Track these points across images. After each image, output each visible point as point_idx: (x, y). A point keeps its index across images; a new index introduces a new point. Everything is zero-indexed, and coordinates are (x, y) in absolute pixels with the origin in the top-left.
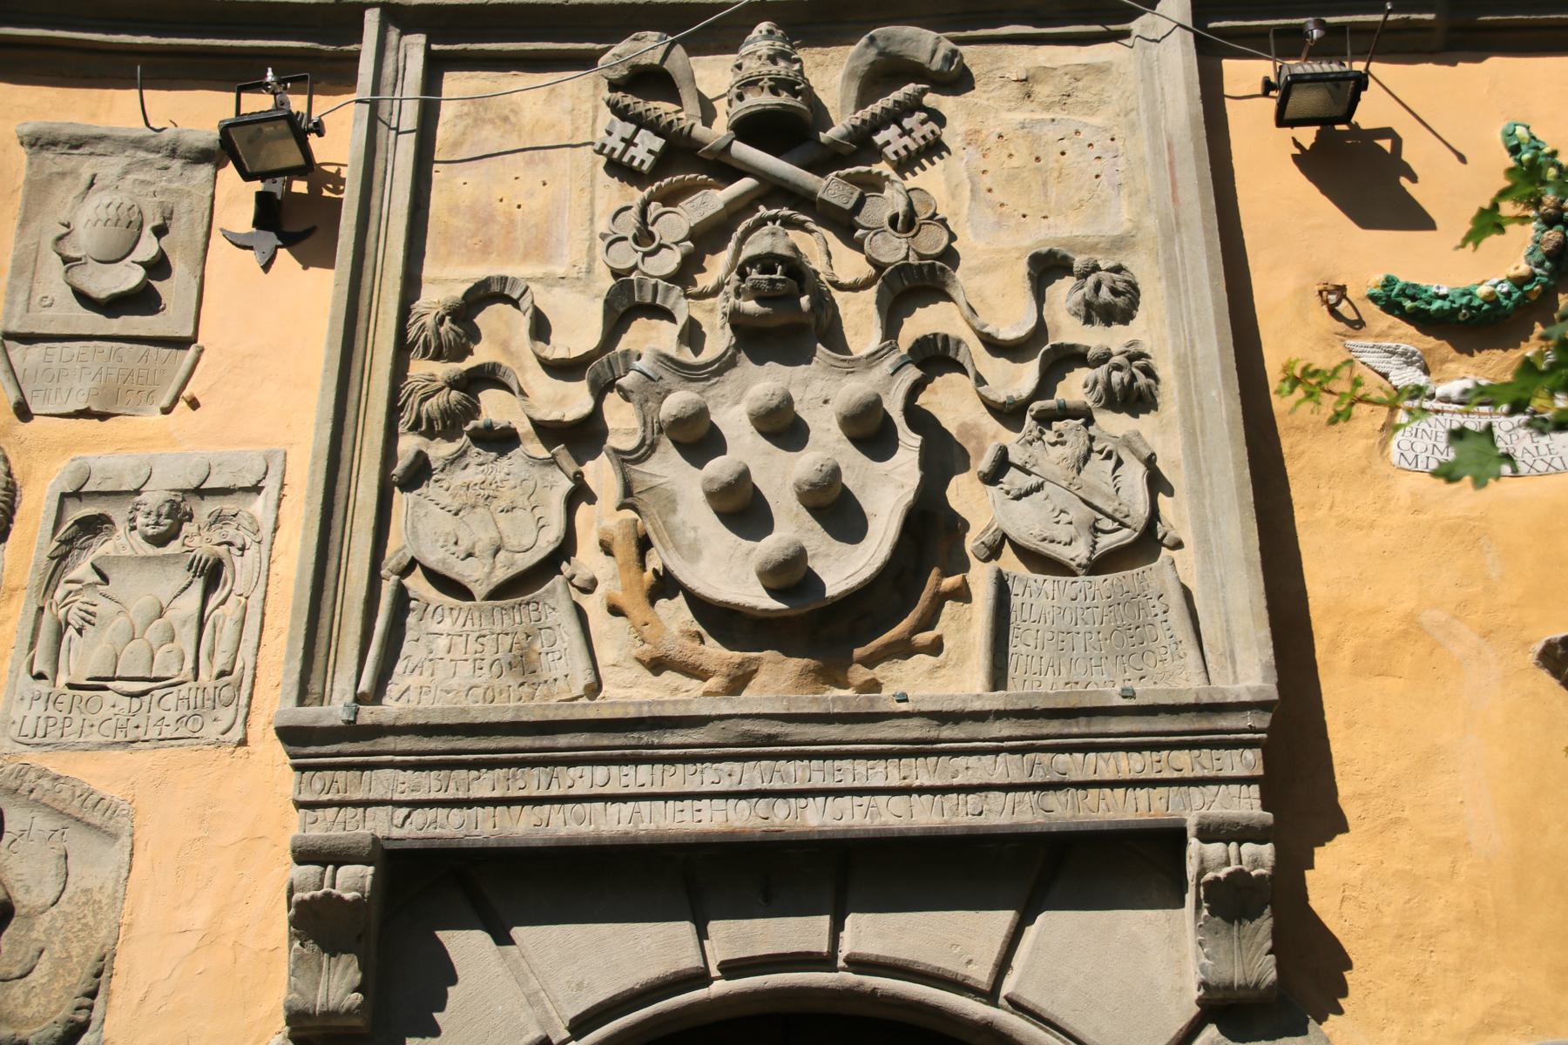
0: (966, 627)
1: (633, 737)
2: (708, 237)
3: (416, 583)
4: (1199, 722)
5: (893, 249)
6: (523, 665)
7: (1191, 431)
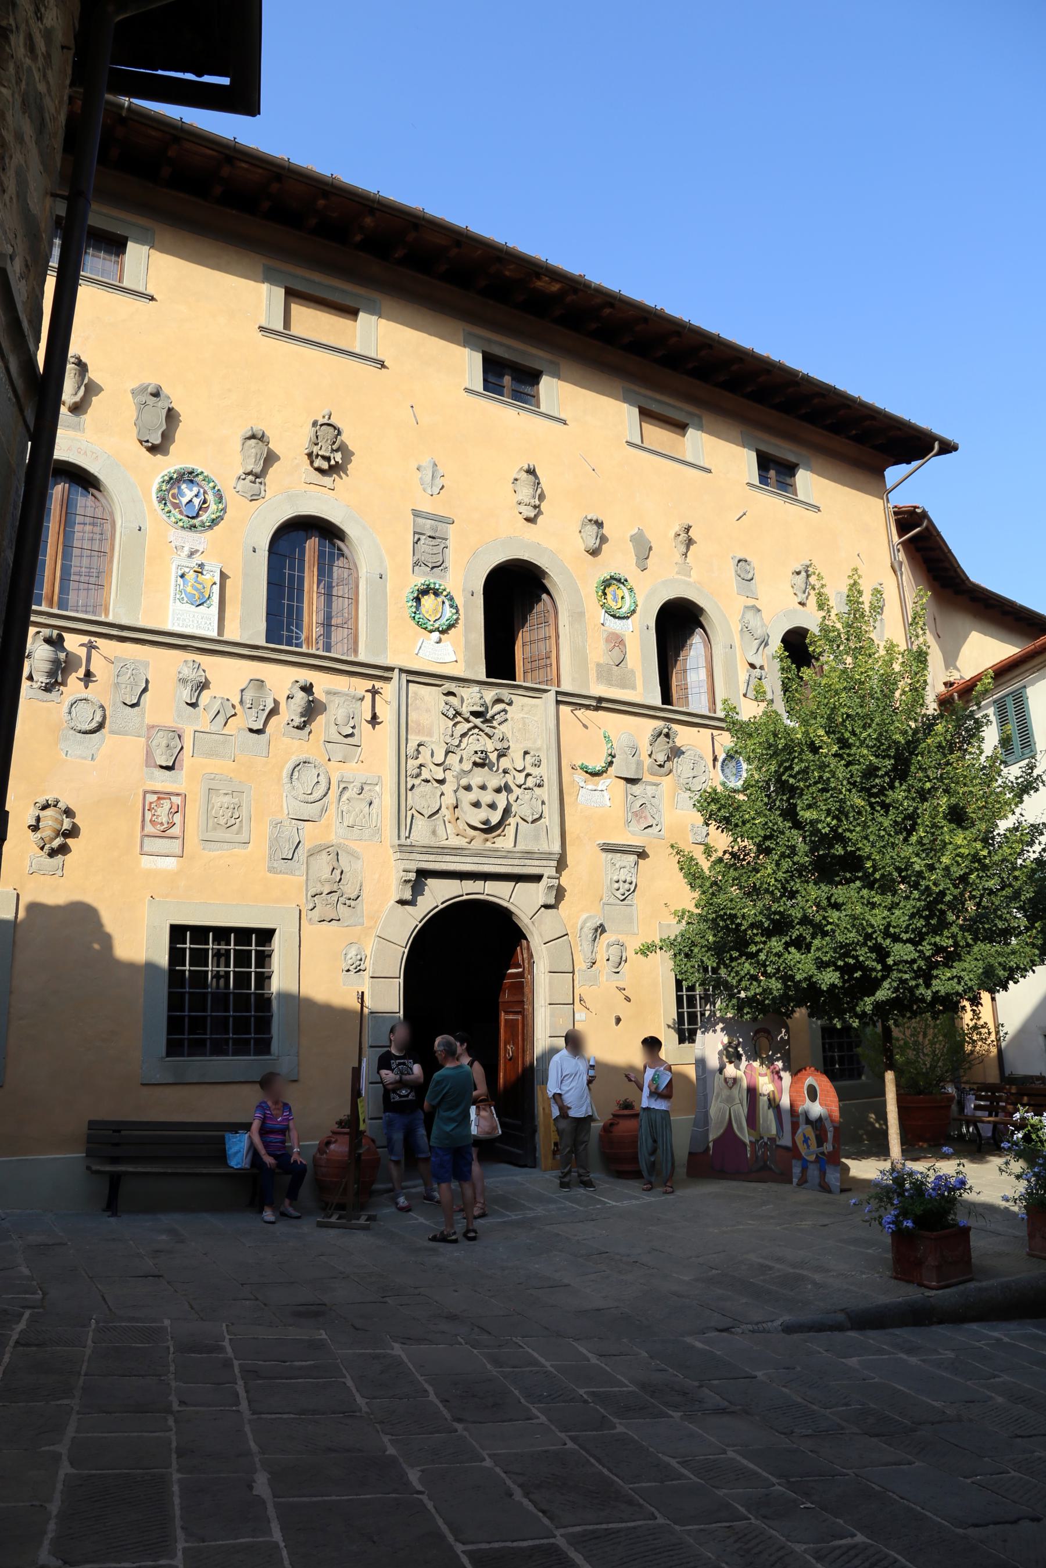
0: (510, 831)
1: (456, 851)
2: (463, 735)
3: (416, 814)
4: (546, 856)
5: (499, 746)
6: (434, 832)
7: (548, 793)
